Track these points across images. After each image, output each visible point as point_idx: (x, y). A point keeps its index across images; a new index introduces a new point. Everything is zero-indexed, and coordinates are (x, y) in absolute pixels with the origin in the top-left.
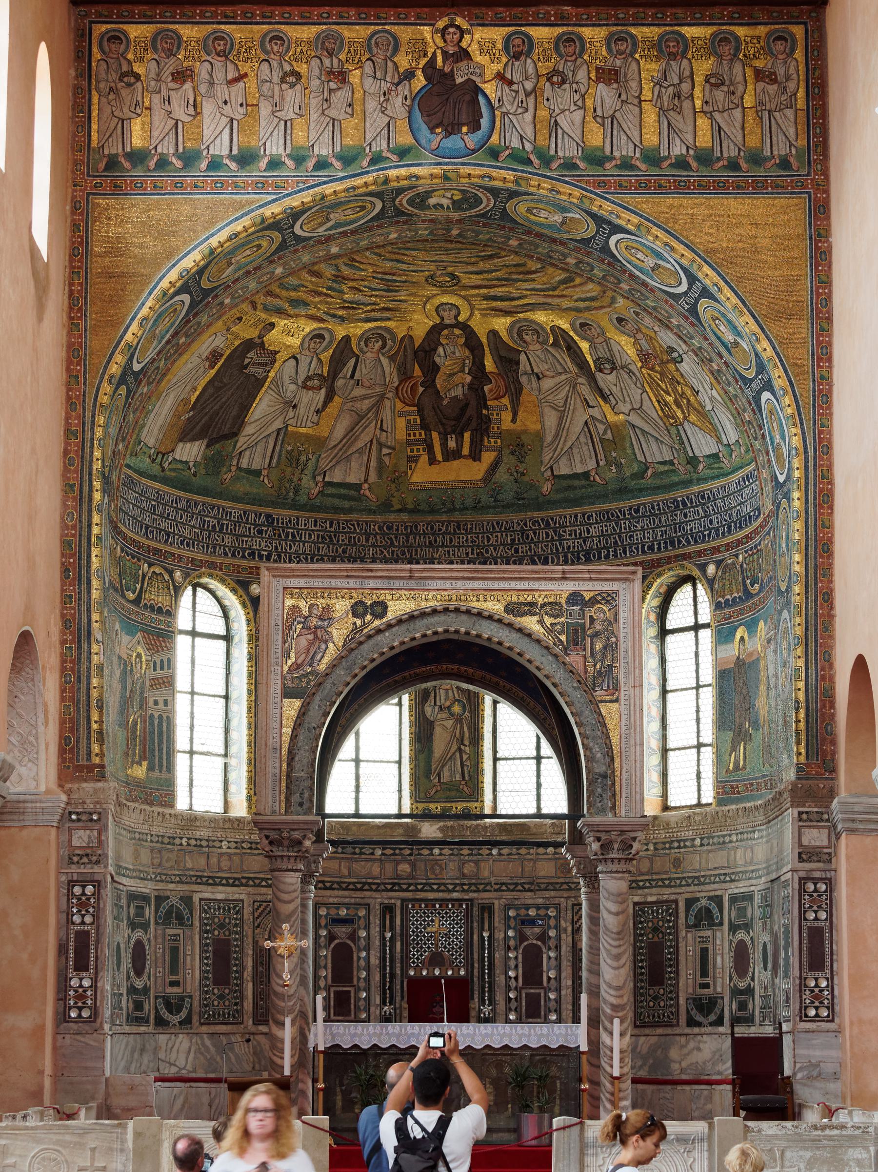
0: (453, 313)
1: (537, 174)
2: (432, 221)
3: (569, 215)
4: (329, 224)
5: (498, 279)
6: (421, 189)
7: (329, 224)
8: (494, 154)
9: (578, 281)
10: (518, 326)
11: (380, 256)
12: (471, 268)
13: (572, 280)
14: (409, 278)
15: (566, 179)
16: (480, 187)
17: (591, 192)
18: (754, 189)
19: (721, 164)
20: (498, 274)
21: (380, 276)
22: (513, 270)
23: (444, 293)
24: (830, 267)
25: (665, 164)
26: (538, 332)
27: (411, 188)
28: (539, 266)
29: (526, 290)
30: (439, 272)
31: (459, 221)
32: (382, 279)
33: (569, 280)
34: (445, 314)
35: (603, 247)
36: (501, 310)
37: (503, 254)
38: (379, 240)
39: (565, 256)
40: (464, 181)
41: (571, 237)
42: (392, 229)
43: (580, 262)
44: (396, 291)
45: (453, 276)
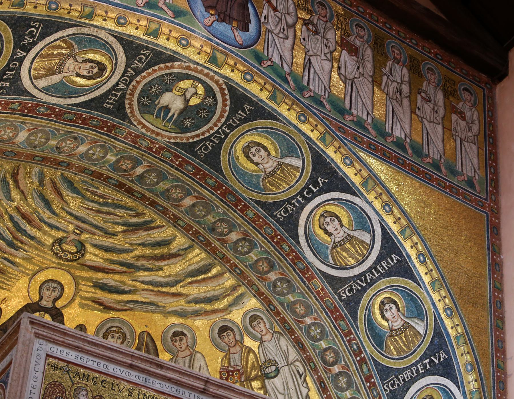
0: (55, 294)
1: (292, 94)
2: (136, 138)
3: (288, 160)
4: (56, 79)
5: (122, 264)
6: (176, 68)
7: (56, 79)
8: (259, 59)
9: (214, 271)
10: (109, 325)
11: (41, 183)
12: (107, 242)
13: (206, 269)
14: (38, 234)
15: (315, 110)
16: (231, 89)
17: (333, 132)
18: (450, 191)
19: (428, 160)
20: (126, 257)
21: (17, 217)
22: (148, 251)
23: (60, 267)
24: (502, 278)
25: (390, 139)
26: (125, 336)
27: (172, 58)
28: (186, 246)
29: (143, 282)
30: (73, 236)
31: (161, 148)
32: (16, 224)
33: (206, 269)
34: (46, 293)
35: (291, 215)
36: (100, 304)
37: (159, 222)
38: (67, 145)
39: (232, 228)
40: (226, 71)
41: (262, 198)
42: (91, 134)
43: (246, 238)
44: (17, 248)
45: (81, 247)
